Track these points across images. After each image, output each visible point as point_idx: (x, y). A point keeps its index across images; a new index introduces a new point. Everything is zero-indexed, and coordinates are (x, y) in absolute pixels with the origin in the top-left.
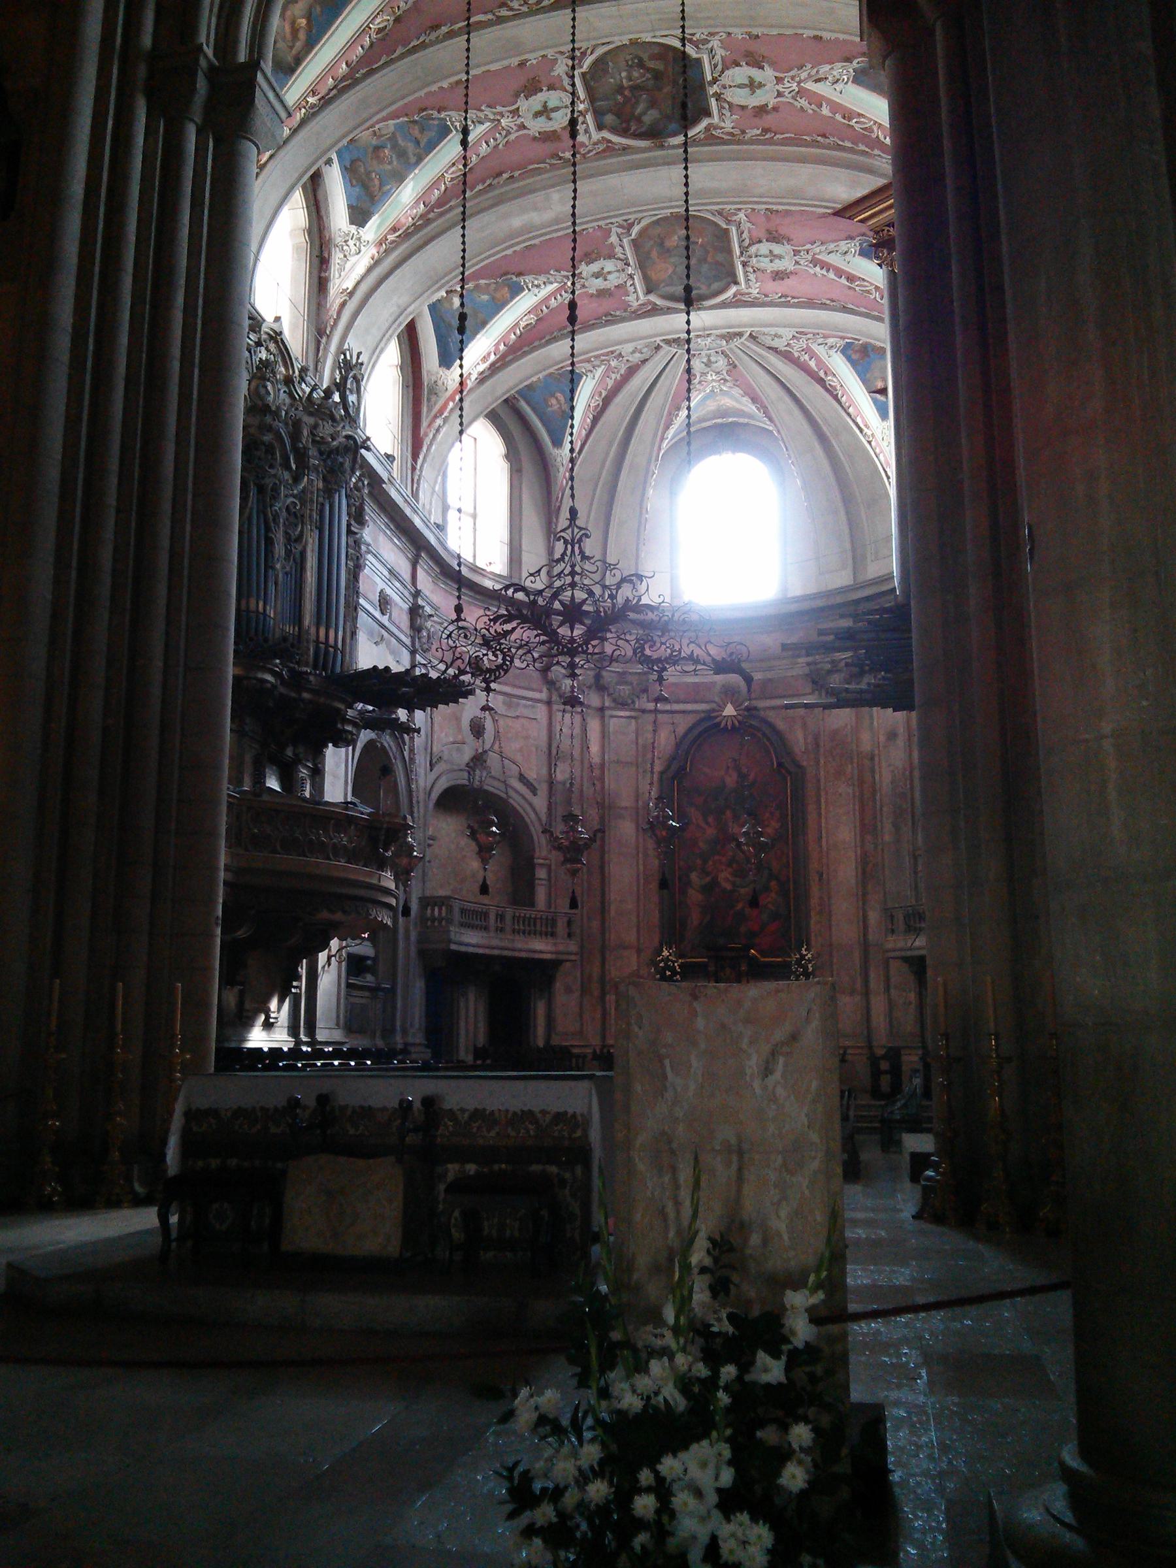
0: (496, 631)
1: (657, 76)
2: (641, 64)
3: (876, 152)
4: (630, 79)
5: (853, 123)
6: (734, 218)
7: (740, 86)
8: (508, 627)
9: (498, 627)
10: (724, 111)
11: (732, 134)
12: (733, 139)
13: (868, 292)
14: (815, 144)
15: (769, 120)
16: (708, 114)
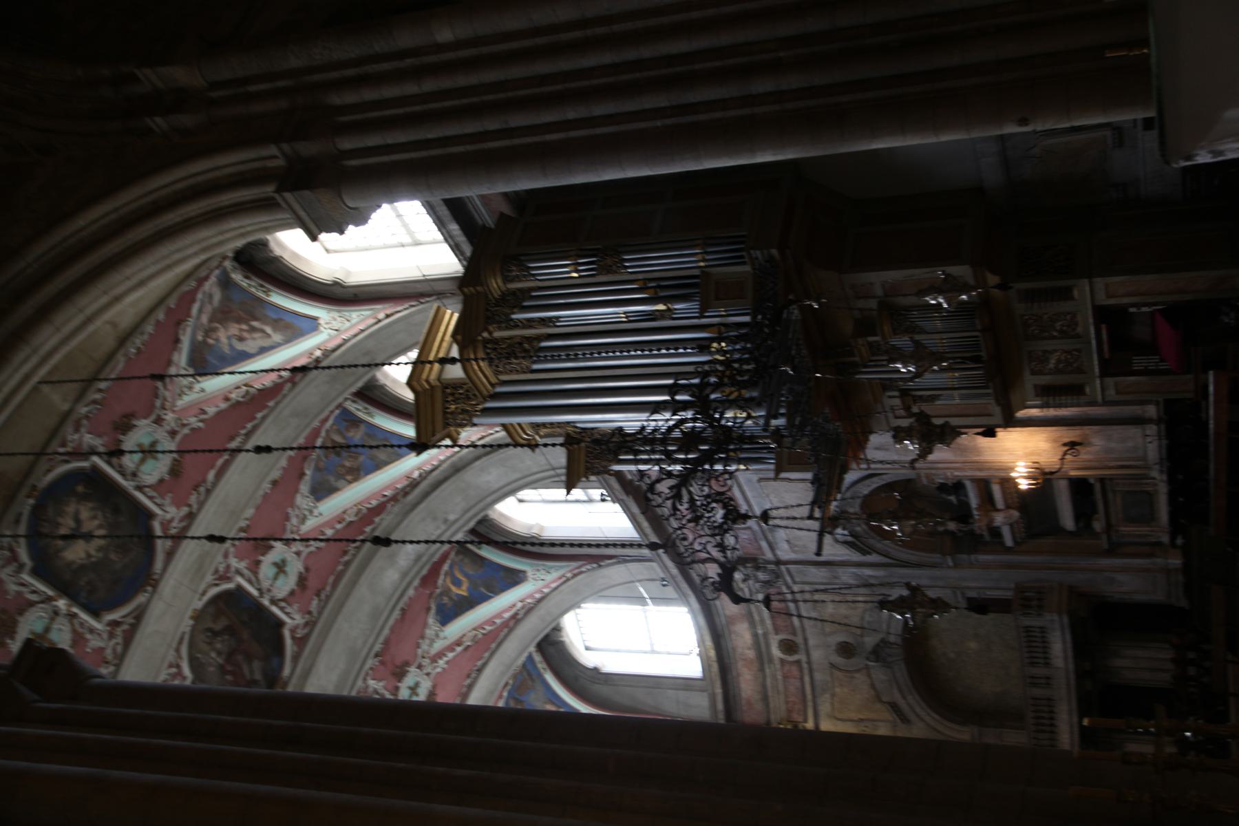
0: (687, 509)
1: (230, 630)
2: (215, 634)
3: (377, 520)
4: (219, 653)
5: (348, 519)
6: (371, 690)
7: (276, 578)
8: (686, 498)
9: (683, 507)
10: (289, 610)
11: (306, 624)
12: (311, 624)
13: (475, 636)
14: (347, 564)
15: (313, 583)
16: (280, 624)
